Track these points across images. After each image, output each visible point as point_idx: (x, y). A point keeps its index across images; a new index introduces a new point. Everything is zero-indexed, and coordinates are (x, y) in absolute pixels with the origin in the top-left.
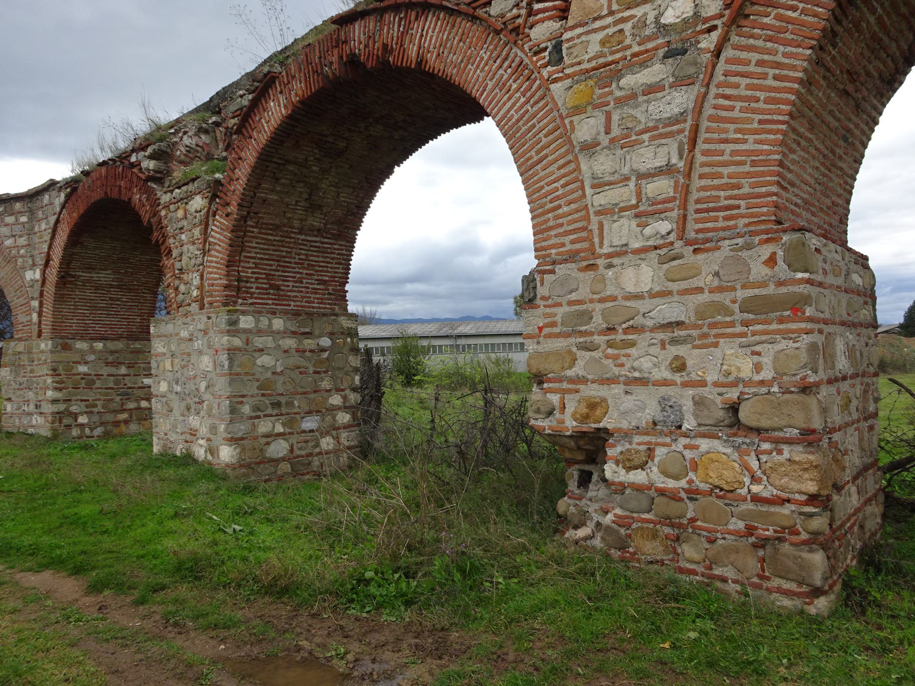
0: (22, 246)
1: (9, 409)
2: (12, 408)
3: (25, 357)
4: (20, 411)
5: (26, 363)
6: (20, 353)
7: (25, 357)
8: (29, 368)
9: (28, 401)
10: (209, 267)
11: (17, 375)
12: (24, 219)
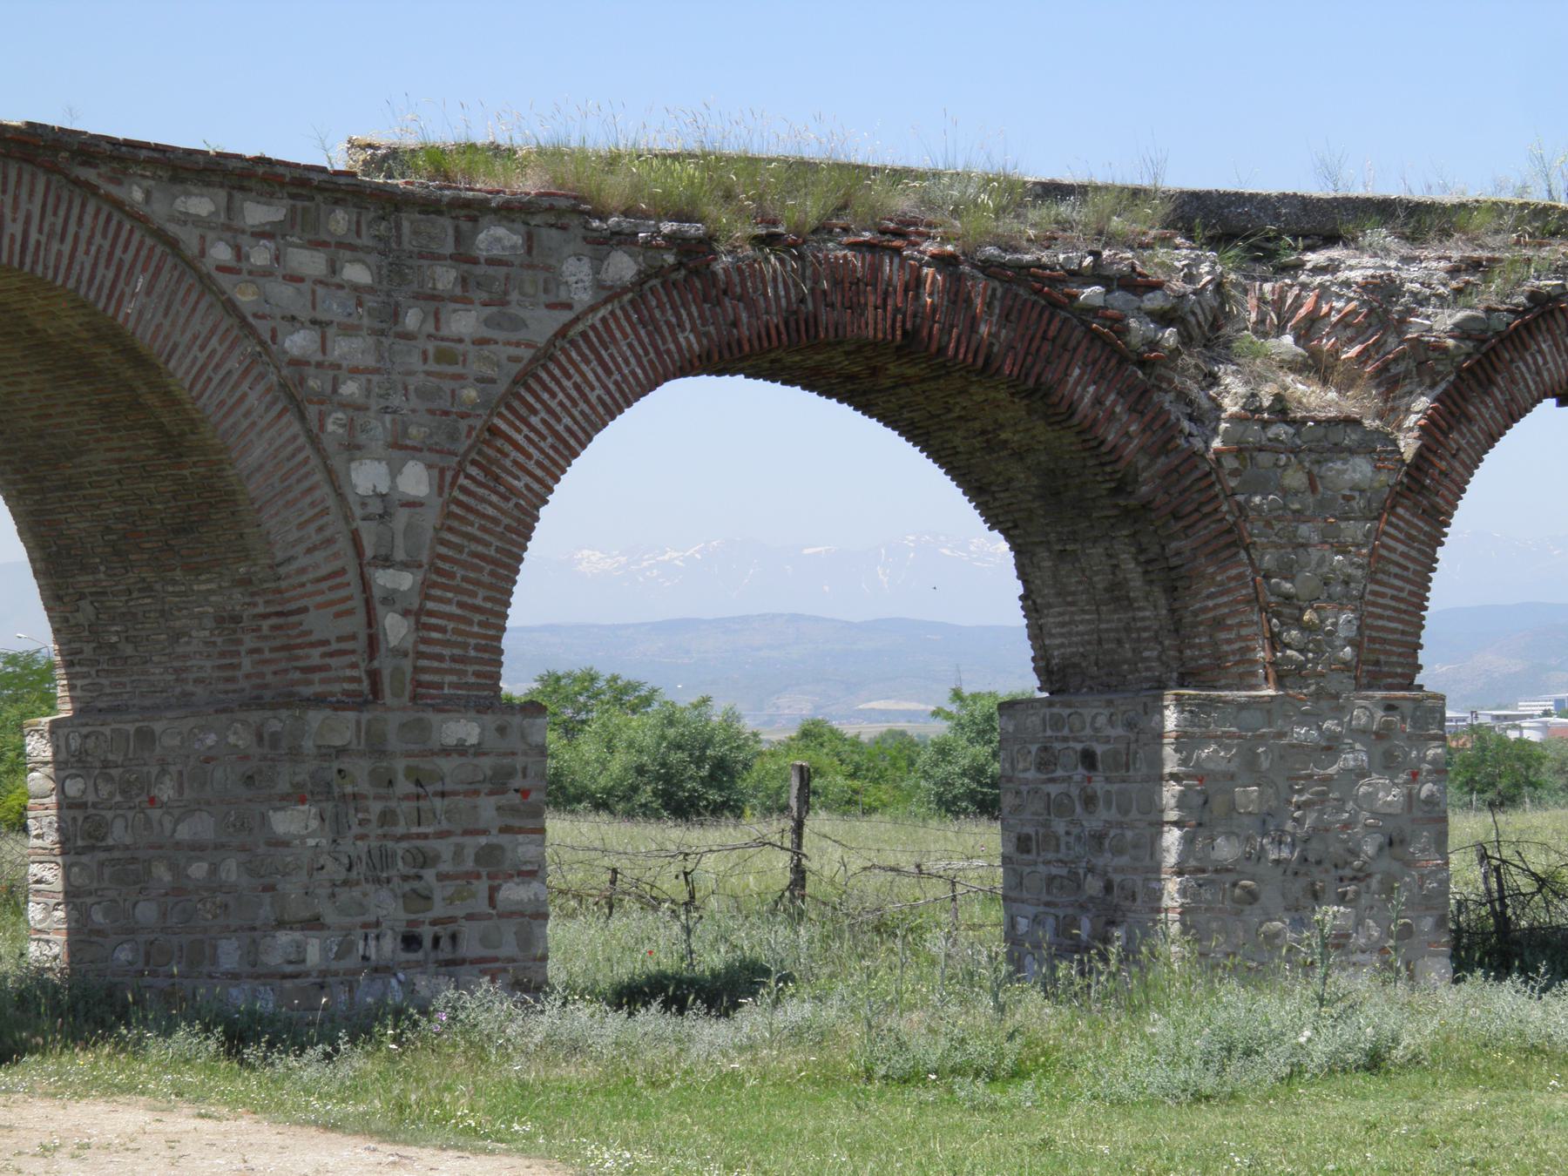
0: (355, 371)
1: (314, 954)
2: (324, 950)
3: (360, 768)
4: (352, 962)
5: (365, 787)
6: (341, 751)
7: (360, 768)
8: (376, 807)
9: (378, 924)
10: (1374, 604)
11: (338, 828)
12: (357, 273)
